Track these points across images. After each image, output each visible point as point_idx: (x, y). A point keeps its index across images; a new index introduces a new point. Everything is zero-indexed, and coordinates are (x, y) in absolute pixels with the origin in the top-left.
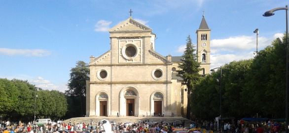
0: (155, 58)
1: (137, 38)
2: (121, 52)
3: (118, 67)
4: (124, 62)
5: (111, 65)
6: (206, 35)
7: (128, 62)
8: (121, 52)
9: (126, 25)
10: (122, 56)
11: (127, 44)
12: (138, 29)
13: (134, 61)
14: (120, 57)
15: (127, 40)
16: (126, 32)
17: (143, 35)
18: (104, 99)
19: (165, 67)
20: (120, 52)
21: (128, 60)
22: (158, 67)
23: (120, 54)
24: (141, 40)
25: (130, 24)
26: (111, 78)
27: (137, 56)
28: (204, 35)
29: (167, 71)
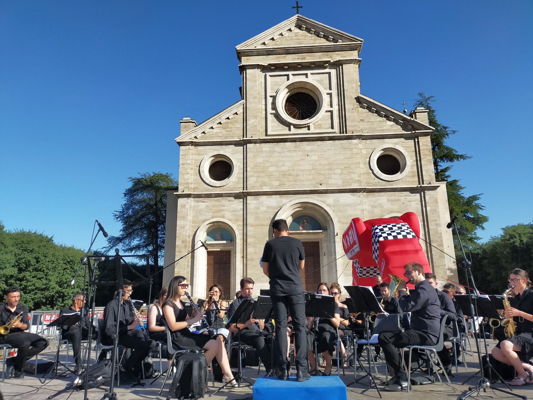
0: (375, 118)
2: (274, 104)
3: (266, 147)
4: (283, 131)
5: (243, 143)
7: (293, 130)
8: (274, 104)
9: (286, 34)
10: (277, 116)
11: (290, 82)
12: (322, 42)
13: (312, 130)
14: (271, 118)
15: (290, 73)
16: (288, 51)
17: (336, 57)
18: (218, 245)
19: (411, 142)
20: (269, 106)
21: (297, 126)
22: (389, 144)
23: (270, 110)
24: (333, 72)
25: (297, 30)
26: (245, 179)
27: (322, 115)
29: (418, 153)
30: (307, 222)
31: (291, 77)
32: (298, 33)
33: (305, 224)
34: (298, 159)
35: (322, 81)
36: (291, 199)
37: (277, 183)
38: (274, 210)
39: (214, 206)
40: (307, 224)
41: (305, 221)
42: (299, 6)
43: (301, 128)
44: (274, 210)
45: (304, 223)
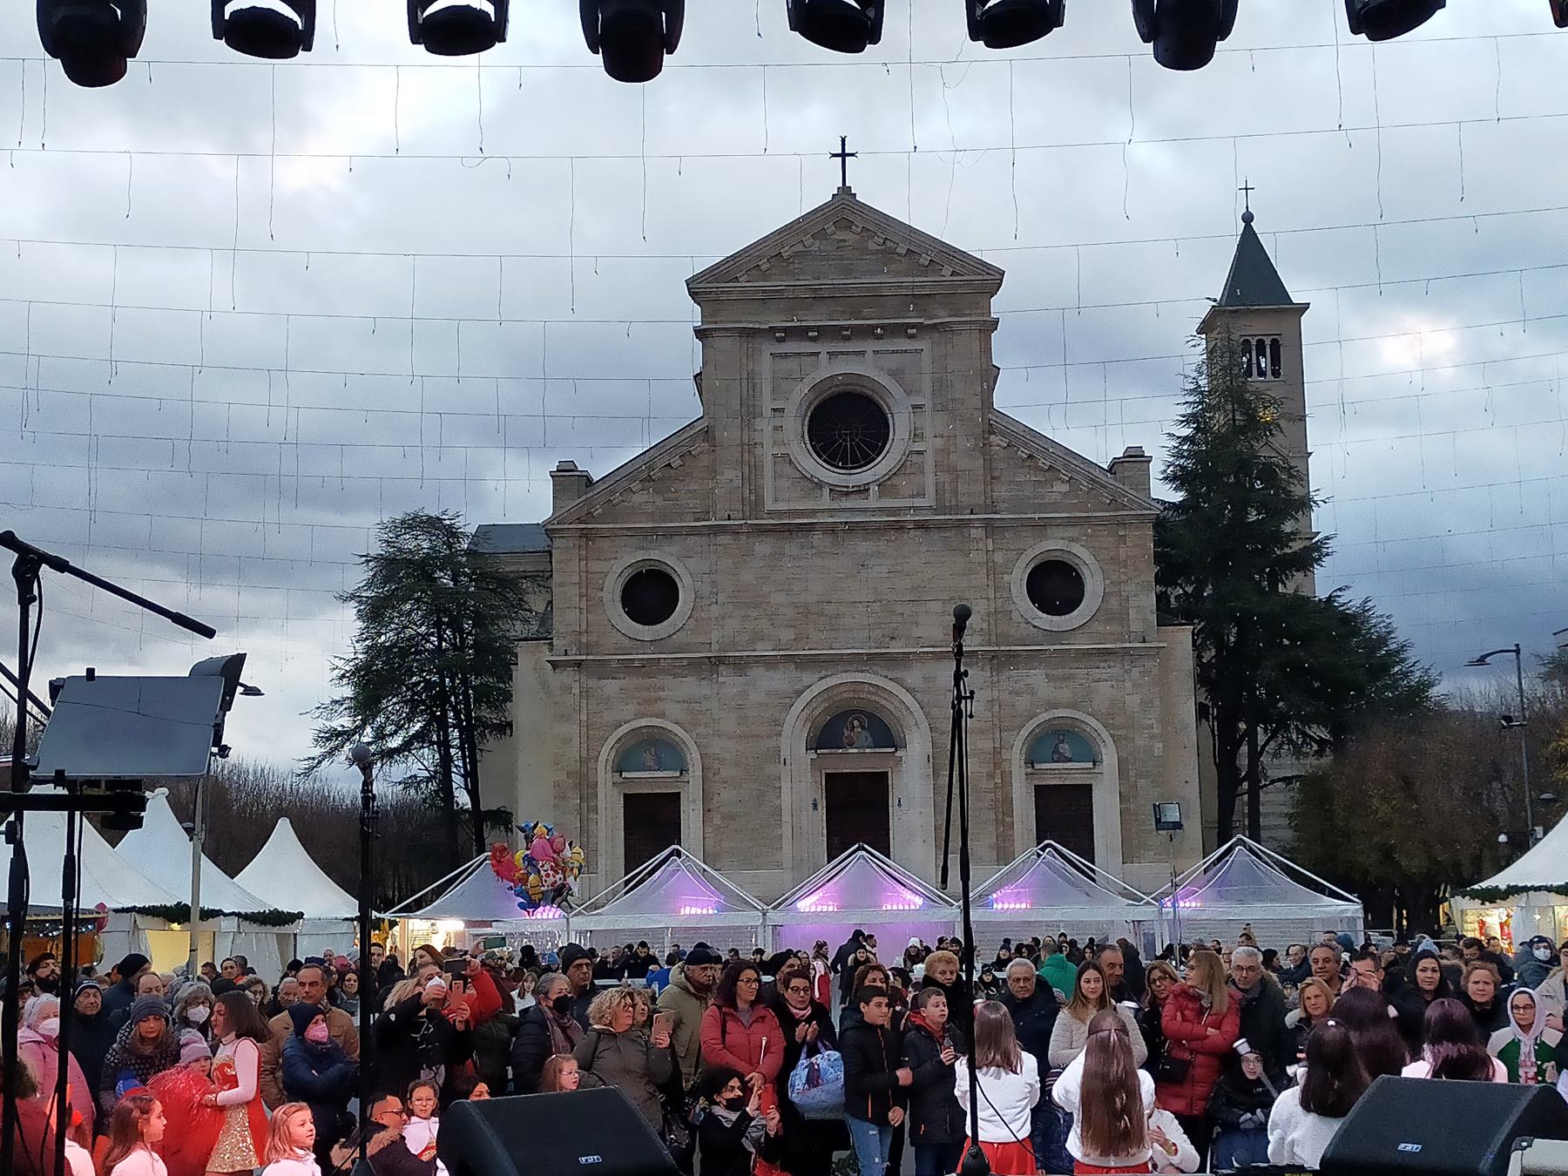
1: (900, 330)
6: (1275, 345)
13: (873, 501)
15: (823, 348)
21: (838, 492)
22: (1053, 544)
25: (840, 235)
28: (1261, 344)
30: (863, 728)
31: (823, 357)
32: (844, 241)
33: (856, 729)
36: (824, 673)
37: (787, 635)
38: (782, 701)
41: (856, 723)
42: (847, 152)
43: (847, 494)
44: (782, 701)
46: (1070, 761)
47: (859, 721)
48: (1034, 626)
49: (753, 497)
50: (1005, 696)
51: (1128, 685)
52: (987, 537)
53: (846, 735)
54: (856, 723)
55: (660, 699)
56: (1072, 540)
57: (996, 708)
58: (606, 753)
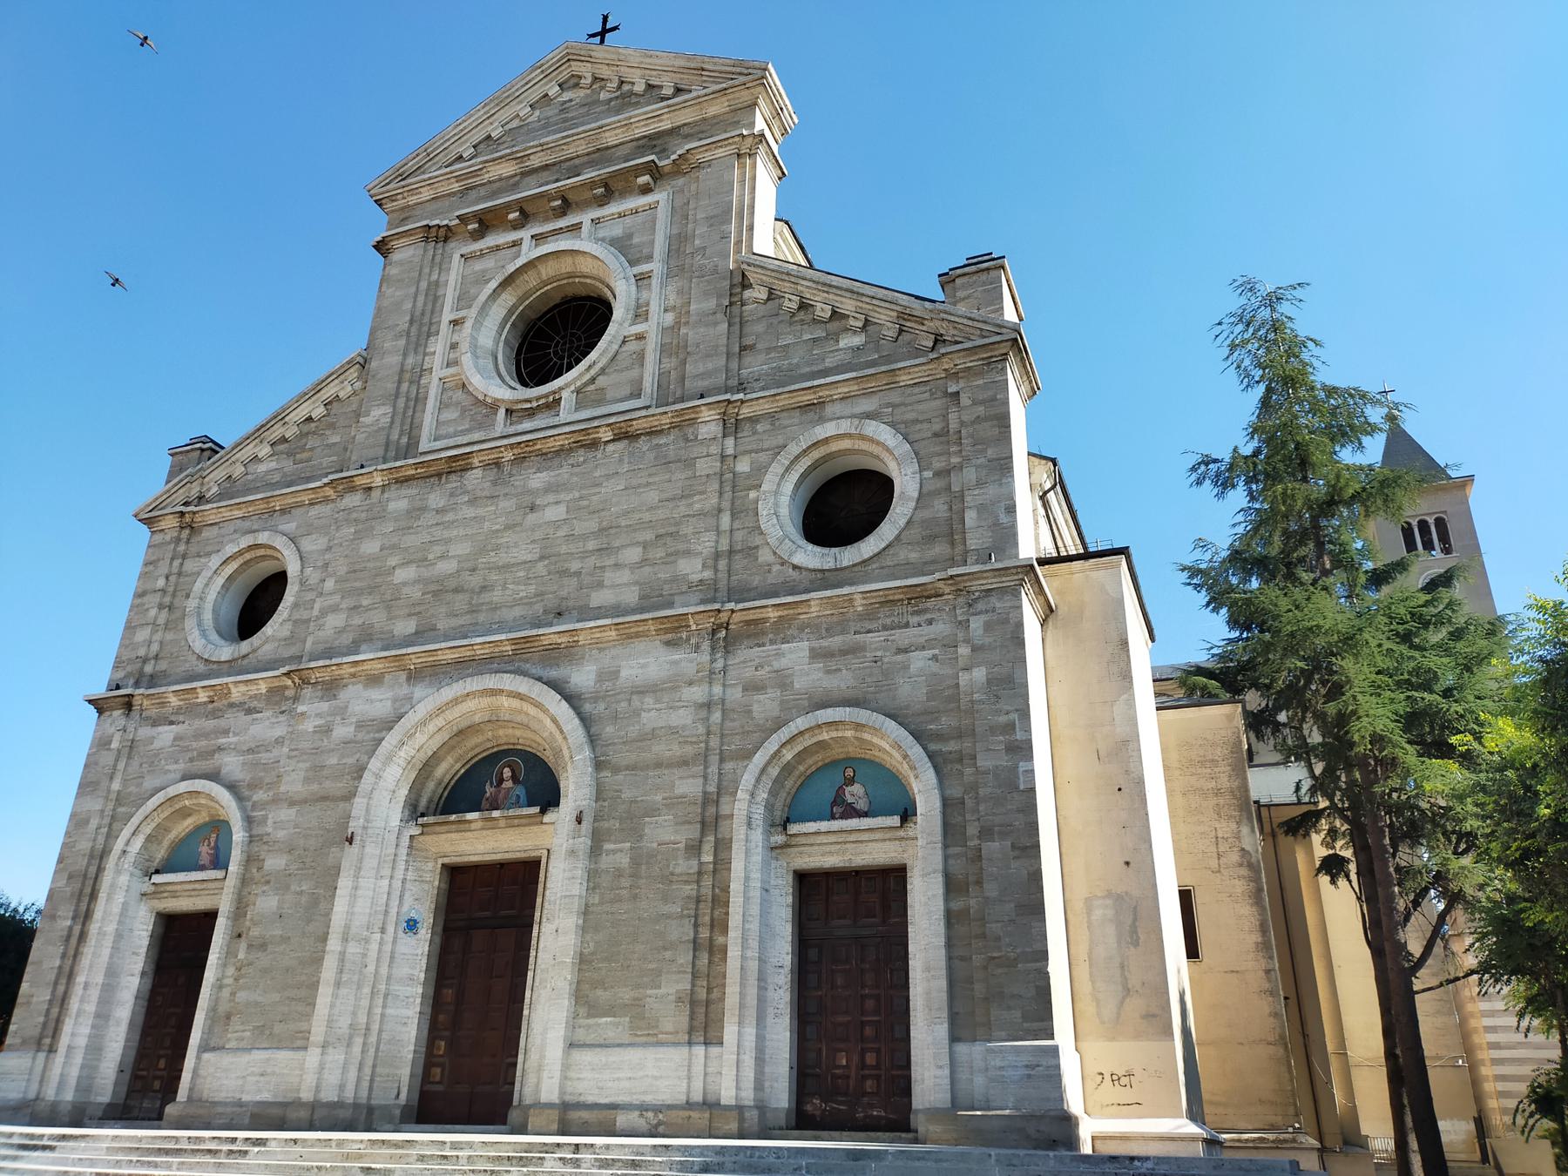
30: (514, 778)
34: (498, 527)
35: (630, 236)
38: (377, 735)
39: (198, 736)
40: (508, 784)
41: (507, 773)
44: (377, 735)
45: (501, 781)
46: (865, 815)
47: (513, 771)
48: (795, 567)
49: (405, 440)
50: (735, 694)
51: (964, 650)
52: (724, 436)
53: (488, 795)
54: (507, 773)
55: (220, 749)
56: (869, 416)
57: (716, 716)
58: (130, 843)
